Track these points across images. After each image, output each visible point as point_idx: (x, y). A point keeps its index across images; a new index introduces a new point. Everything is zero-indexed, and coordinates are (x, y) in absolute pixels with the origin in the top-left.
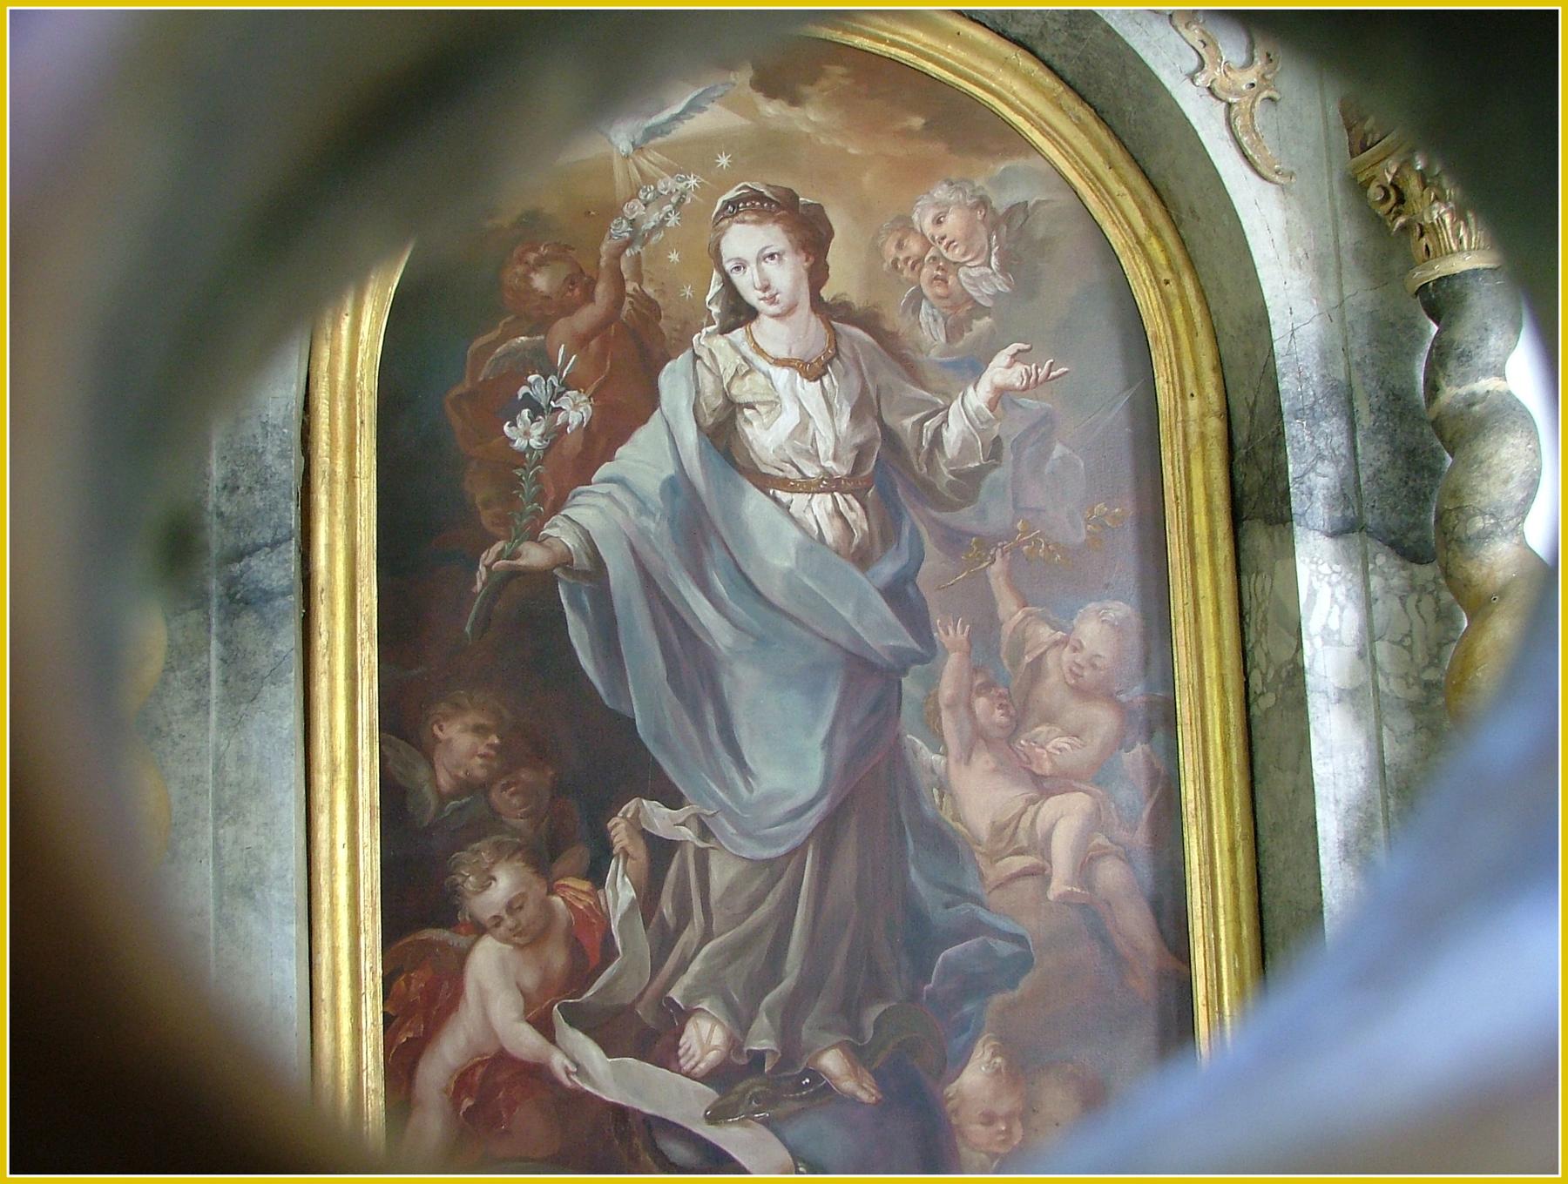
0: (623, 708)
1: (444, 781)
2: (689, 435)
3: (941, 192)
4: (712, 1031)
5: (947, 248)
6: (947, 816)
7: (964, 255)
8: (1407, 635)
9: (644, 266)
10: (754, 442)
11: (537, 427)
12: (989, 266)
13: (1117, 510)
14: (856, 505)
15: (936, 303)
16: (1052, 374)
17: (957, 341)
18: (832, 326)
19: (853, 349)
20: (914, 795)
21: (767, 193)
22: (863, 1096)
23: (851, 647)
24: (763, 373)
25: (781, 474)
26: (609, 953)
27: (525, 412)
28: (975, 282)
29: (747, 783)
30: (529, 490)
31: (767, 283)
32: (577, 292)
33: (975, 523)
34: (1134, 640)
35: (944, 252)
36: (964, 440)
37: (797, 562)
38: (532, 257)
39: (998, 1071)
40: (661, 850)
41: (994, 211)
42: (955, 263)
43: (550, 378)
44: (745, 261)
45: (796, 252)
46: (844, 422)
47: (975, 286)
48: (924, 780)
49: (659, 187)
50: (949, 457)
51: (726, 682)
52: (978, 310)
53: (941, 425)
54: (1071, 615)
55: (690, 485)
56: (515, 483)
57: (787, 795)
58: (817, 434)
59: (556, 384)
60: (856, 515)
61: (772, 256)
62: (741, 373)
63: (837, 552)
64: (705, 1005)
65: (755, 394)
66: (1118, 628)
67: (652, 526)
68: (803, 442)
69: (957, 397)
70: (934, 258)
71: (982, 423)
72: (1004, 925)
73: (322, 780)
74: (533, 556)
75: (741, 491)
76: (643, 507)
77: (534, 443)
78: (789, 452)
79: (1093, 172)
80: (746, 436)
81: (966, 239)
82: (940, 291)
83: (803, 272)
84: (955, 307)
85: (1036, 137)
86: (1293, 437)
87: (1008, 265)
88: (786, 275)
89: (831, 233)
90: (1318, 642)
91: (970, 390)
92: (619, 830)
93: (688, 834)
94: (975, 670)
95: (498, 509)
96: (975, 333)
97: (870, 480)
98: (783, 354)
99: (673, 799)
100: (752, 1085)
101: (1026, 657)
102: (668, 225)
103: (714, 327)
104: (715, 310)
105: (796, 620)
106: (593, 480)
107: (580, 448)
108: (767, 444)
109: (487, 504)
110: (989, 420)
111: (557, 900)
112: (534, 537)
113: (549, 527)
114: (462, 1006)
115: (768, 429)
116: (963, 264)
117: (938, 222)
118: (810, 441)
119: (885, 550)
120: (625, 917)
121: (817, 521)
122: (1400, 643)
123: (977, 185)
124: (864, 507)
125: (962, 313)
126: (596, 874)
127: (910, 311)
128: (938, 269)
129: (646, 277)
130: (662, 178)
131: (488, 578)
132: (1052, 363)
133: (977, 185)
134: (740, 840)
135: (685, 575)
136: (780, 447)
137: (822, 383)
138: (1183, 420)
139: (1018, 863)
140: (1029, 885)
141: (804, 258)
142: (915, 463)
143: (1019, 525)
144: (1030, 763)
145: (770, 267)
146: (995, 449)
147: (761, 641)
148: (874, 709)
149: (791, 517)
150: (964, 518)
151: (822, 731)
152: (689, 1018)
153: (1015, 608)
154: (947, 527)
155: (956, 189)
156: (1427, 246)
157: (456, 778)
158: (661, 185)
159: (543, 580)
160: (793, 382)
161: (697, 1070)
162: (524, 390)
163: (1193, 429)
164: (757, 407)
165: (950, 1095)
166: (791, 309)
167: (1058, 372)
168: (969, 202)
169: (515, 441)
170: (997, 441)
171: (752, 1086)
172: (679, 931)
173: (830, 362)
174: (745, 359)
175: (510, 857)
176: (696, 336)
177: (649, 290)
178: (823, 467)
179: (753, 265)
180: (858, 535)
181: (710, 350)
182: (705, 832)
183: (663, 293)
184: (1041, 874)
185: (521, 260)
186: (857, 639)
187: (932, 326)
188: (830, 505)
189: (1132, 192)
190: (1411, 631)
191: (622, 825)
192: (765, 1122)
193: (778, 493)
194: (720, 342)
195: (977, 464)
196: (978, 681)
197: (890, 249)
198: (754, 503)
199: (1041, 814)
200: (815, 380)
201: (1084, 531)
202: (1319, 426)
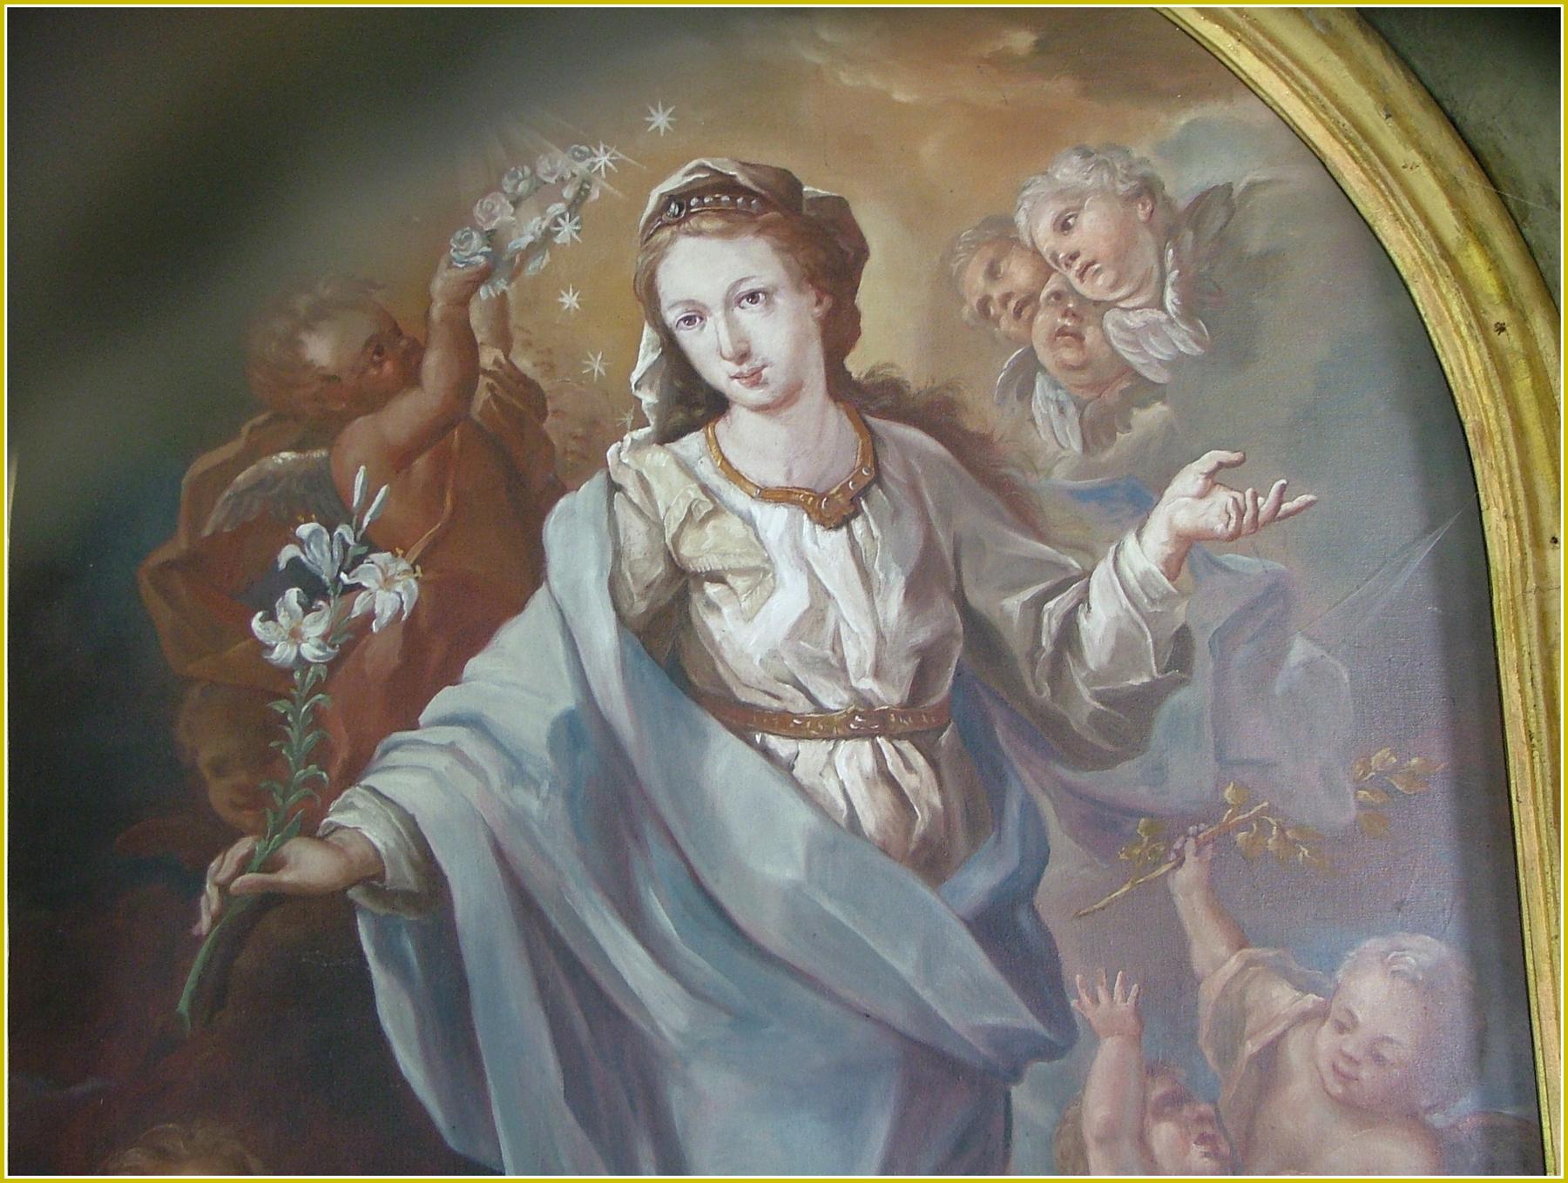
3: (1068, 171)
5: (1082, 274)
7: (1115, 286)
9: (514, 318)
10: (725, 645)
11: (316, 622)
12: (1161, 306)
13: (1414, 761)
14: (918, 760)
15: (1061, 378)
16: (1286, 506)
17: (1105, 448)
18: (868, 427)
21: (742, 179)
23: (912, 1029)
24: (740, 515)
25: (775, 704)
27: (293, 594)
28: (1135, 338)
30: (300, 739)
31: (743, 347)
33: (1143, 790)
34: (1454, 1007)
35: (1076, 282)
36: (1121, 636)
37: (809, 868)
38: (302, 303)
41: (1168, 203)
42: (1097, 303)
43: (339, 530)
44: (705, 307)
45: (799, 289)
46: (893, 605)
47: (1136, 344)
50: (1092, 665)
51: (676, 1097)
52: (1142, 390)
53: (1074, 610)
54: (1332, 961)
55: (606, 728)
56: (273, 727)
58: (842, 625)
59: (350, 541)
60: (918, 779)
61: (753, 296)
62: (698, 517)
63: (884, 849)
66: (1425, 986)
67: (534, 805)
68: (817, 644)
69: (1105, 556)
70: (1057, 295)
71: (1153, 601)
75: (700, 736)
76: (517, 770)
77: (310, 650)
78: (790, 663)
79: (1357, 124)
80: (710, 636)
82: (1069, 355)
83: (813, 328)
84: (1099, 386)
85: (1247, 62)
89: (863, 253)
91: (1130, 541)
94: (1151, 1071)
95: (242, 778)
96: (1137, 432)
97: (944, 714)
98: (775, 478)
101: (1249, 1045)
102: (558, 240)
103: (647, 430)
104: (648, 398)
105: (808, 980)
106: (423, 719)
107: (395, 661)
108: (750, 648)
109: (219, 769)
110: (1166, 598)
112: (310, 828)
113: (340, 810)
115: (749, 620)
116: (1112, 305)
118: (829, 642)
119: (974, 845)
123: (1136, 155)
124: (933, 764)
125: (1111, 397)
127: (1013, 395)
128: (1065, 315)
129: (518, 336)
132: (1283, 487)
133: (1136, 155)
135: (597, 896)
136: (774, 654)
141: (814, 299)
142: (1028, 680)
143: (1228, 793)
145: (750, 317)
147: (743, 1021)
153: (1222, 950)
155: (1098, 164)
158: (543, 167)
160: (794, 530)
162: (289, 552)
164: (729, 578)
166: (790, 396)
167: (1295, 504)
168: (1122, 188)
169: (272, 648)
173: (864, 492)
174: (705, 489)
176: (613, 449)
177: (524, 364)
179: (718, 313)
183: (550, 368)
186: (924, 1013)
187: (1056, 423)
188: (868, 762)
189: (1431, 159)
193: (773, 742)
194: (658, 458)
195: (1146, 679)
196: (1158, 1090)
197: (975, 281)
200: (837, 527)
201: (1352, 803)
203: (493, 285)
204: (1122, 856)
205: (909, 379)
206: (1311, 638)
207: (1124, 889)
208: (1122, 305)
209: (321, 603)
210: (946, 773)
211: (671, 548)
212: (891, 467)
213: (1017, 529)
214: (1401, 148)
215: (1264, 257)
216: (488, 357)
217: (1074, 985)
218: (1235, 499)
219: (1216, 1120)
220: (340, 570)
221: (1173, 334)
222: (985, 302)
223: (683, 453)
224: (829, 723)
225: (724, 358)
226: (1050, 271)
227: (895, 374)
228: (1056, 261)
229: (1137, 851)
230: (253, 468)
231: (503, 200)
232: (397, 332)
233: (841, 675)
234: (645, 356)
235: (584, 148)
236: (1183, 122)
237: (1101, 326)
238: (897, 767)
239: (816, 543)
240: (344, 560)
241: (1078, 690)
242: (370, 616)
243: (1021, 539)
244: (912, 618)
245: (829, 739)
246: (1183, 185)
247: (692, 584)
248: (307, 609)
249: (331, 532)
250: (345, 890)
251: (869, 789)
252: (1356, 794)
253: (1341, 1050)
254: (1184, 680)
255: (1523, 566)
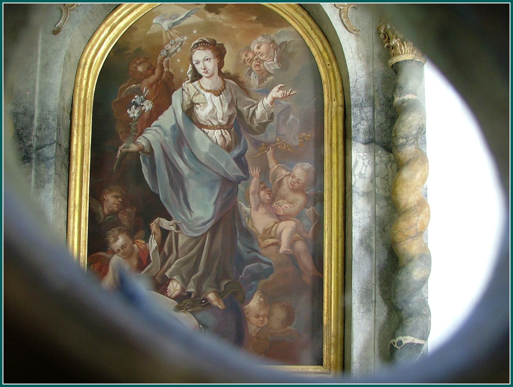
0: (156, 192)
1: (106, 211)
2: (180, 112)
3: (260, 39)
4: (177, 285)
5: (261, 56)
6: (250, 226)
7: (266, 58)
8: (386, 176)
9: (170, 64)
10: (199, 115)
11: (137, 111)
12: (274, 61)
13: (309, 135)
14: (228, 133)
15: (256, 72)
17: (262, 84)
18: (224, 80)
19: (230, 86)
20: (240, 220)
21: (207, 41)
22: (220, 307)
23: (223, 175)
24: (203, 94)
25: (206, 124)
26: (149, 261)
27: (134, 106)
28: (269, 66)
29: (191, 214)
30: (133, 128)
31: (205, 68)
32: (150, 71)
33: (264, 139)
34: (311, 175)
35: (260, 57)
36: (262, 114)
38: (138, 61)
39: (261, 303)
40: (165, 233)
41: (276, 44)
42: (263, 60)
43: (141, 97)
44: (200, 61)
45: (215, 58)
46: (226, 108)
48: (243, 215)
49: (176, 40)
50: (257, 118)
51: (186, 185)
52: (269, 74)
53: (255, 110)
54: (292, 167)
56: (130, 127)
57: (202, 218)
58: (217, 112)
59: (143, 98)
60: (228, 136)
62: (196, 94)
63: (221, 147)
64: (175, 278)
65: (200, 100)
66: (307, 171)
67: (168, 139)
68: (213, 114)
69: (261, 101)
70: (256, 59)
71: (268, 108)
72: (266, 259)
73: (71, 209)
74: (133, 148)
75: (194, 129)
76: (165, 134)
77: (136, 115)
79: (307, 32)
81: (267, 53)
82: (258, 69)
83: (217, 64)
84: (262, 73)
85: (290, 21)
86: (354, 113)
87: (280, 60)
88: (211, 65)
89: (225, 52)
90: (357, 177)
91: (265, 99)
92: (153, 226)
93: (173, 228)
94: (261, 183)
95: (125, 135)
96: (268, 81)
97: (232, 126)
98: (209, 89)
99: (169, 218)
100: (188, 301)
101: (277, 180)
102: (178, 51)
103: (189, 81)
104: (190, 76)
106: (151, 126)
107: (148, 117)
108: (203, 115)
110: (270, 108)
111: (135, 246)
112: (134, 142)
113: (138, 139)
114: (108, 274)
115: (203, 111)
116: (265, 61)
117: (258, 48)
118: (215, 115)
119: (236, 147)
120: (154, 251)
121: (216, 138)
122: (384, 178)
123: (271, 36)
124: (230, 133)
125: (264, 75)
126: (146, 239)
127: (248, 75)
128: (257, 62)
129: (170, 66)
130: (176, 37)
131: (121, 154)
132: (291, 90)
133: (271, 36)
134: (188, 231)
135: (176, 153)
136: (206, 116)
137: (220, 97)
138: (331, 107)
139: (271, 241)
140: (274, 248)
141: (217, 60)
142: (246, 120)
144: (276, 211)
145: (207, 63)
146: (271, 117)
147: (197, 173)
148: (229, 194)
149: (208, 136)
150: (261, 137)
151: (213, 200)
152: (170, 281)
153: (274, 164)
154: (255, 140)
155: (265, 38)
156: (393, 53)
157: (109, 210)
158: (176, 40)
159: (137, 154)
161: (172, 296)
162: (134, 100)
163: (334, 110)
164: (200, 104)
165: (246, 308)
166: (212, 75)
167: (293, 93)
168: (269, 42)
169: (130, 115)
170: (273, 113)
171: (188, 301)
172: (169, 256)
173: (223, 90)
174: (197, 90)
175: (123, 233)
176: (184, 84)
177: (171, 70)
178: (218, 122)
180: (228, 142)
181: (187, 88)
182: (178, 228)
184: (278, 245)
185: (135, 62)
186: (225, 173)
187: (254, 79)
188: (220, 133)
189: (319, 37)
190: (388, 175)
191: (154, 225)
192: (191, 312)
193: (205, 130)
194: (191, 85)
195: (266, 121)
196: (262, 186)
197: (243, 57)
198: (198, 132)
199: (279, 226)
200: (218, 96)
201: (298, 142)
202: (363, 109)
203: (167, 59)
204: (260, 149)
205: (231, 72)
206: (293, 114)
207: (259, 154)
208: (267, 61)
209: (138, 108)
210: (232, 136)
211: (191, 99)
212: (227, 87)
213: (247, 97)
214: (314, 35)
215: (291, 53)
216: (165, 70)
217: (250, 169)
218: (283, 92)
219: (271, 191)
220: (141, 103)
221: (275, 65)
222: (245, 60)
223: (195, 84)
224: (214, 127)
225: (202, 69)
226: (256, 55)
227: (229, 72)
228: (257, 53)
229: (262, 148)
230: (129, 87)
231: (170, 45)
232: (152, 66)
233: (217, 119)
234: (190, 69)
235: (183, 37)
236: (280, 31)
237: (263, 64)
238: (224, 134)
239: (214, 98)
240: (141, 102)
241: (254, 123)
242: (145, 110)
243: (247, 98)
244: (229, 111)
245: (214, 129)
246: (278, 41)
247: (194, 105)
248: (135, 109)
249: (140, 97)
250: (138, 152)
251: (220, 138)
252: (299, 140)
253: (292, 181)
254: (272, 121)
255: (329, 104)
